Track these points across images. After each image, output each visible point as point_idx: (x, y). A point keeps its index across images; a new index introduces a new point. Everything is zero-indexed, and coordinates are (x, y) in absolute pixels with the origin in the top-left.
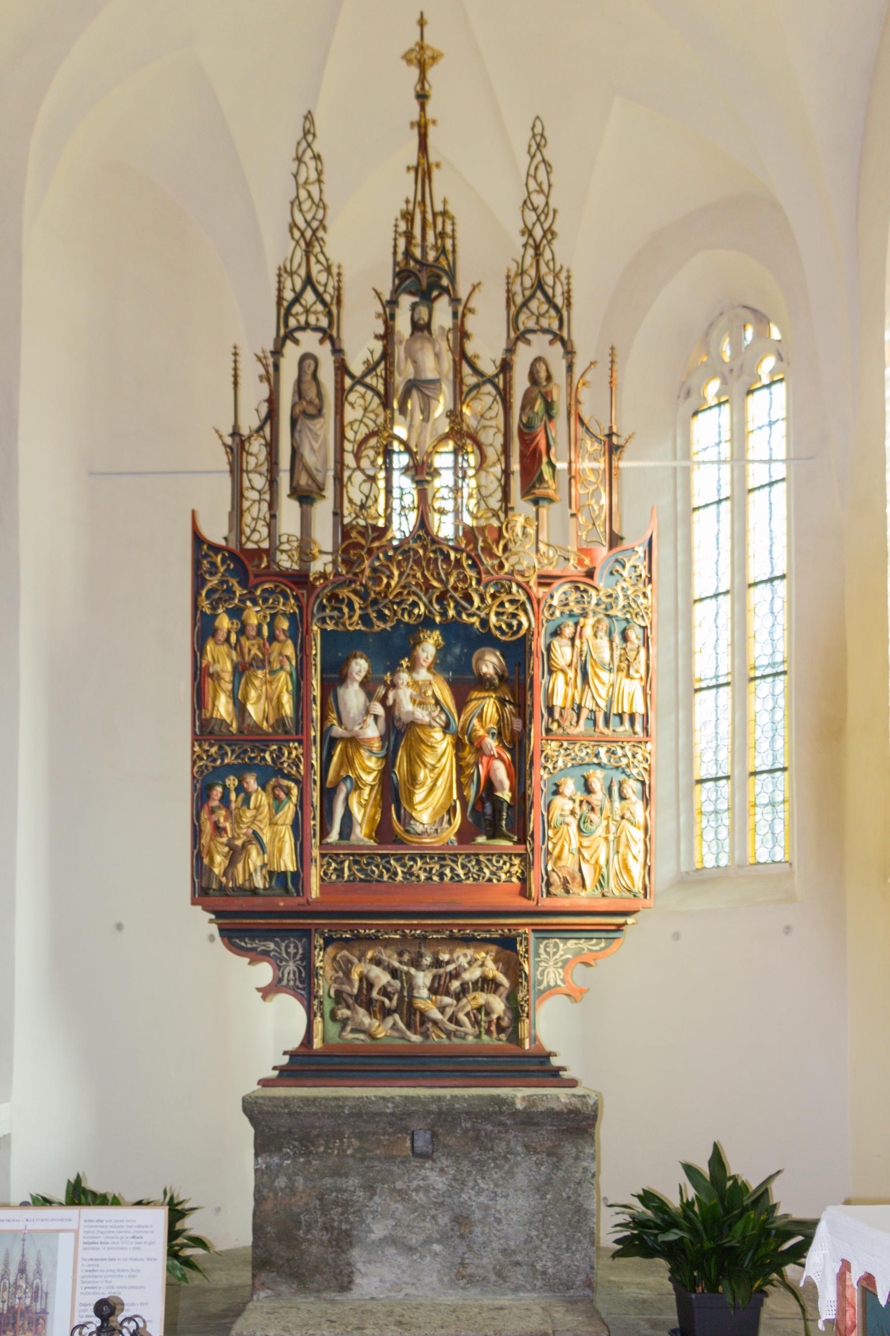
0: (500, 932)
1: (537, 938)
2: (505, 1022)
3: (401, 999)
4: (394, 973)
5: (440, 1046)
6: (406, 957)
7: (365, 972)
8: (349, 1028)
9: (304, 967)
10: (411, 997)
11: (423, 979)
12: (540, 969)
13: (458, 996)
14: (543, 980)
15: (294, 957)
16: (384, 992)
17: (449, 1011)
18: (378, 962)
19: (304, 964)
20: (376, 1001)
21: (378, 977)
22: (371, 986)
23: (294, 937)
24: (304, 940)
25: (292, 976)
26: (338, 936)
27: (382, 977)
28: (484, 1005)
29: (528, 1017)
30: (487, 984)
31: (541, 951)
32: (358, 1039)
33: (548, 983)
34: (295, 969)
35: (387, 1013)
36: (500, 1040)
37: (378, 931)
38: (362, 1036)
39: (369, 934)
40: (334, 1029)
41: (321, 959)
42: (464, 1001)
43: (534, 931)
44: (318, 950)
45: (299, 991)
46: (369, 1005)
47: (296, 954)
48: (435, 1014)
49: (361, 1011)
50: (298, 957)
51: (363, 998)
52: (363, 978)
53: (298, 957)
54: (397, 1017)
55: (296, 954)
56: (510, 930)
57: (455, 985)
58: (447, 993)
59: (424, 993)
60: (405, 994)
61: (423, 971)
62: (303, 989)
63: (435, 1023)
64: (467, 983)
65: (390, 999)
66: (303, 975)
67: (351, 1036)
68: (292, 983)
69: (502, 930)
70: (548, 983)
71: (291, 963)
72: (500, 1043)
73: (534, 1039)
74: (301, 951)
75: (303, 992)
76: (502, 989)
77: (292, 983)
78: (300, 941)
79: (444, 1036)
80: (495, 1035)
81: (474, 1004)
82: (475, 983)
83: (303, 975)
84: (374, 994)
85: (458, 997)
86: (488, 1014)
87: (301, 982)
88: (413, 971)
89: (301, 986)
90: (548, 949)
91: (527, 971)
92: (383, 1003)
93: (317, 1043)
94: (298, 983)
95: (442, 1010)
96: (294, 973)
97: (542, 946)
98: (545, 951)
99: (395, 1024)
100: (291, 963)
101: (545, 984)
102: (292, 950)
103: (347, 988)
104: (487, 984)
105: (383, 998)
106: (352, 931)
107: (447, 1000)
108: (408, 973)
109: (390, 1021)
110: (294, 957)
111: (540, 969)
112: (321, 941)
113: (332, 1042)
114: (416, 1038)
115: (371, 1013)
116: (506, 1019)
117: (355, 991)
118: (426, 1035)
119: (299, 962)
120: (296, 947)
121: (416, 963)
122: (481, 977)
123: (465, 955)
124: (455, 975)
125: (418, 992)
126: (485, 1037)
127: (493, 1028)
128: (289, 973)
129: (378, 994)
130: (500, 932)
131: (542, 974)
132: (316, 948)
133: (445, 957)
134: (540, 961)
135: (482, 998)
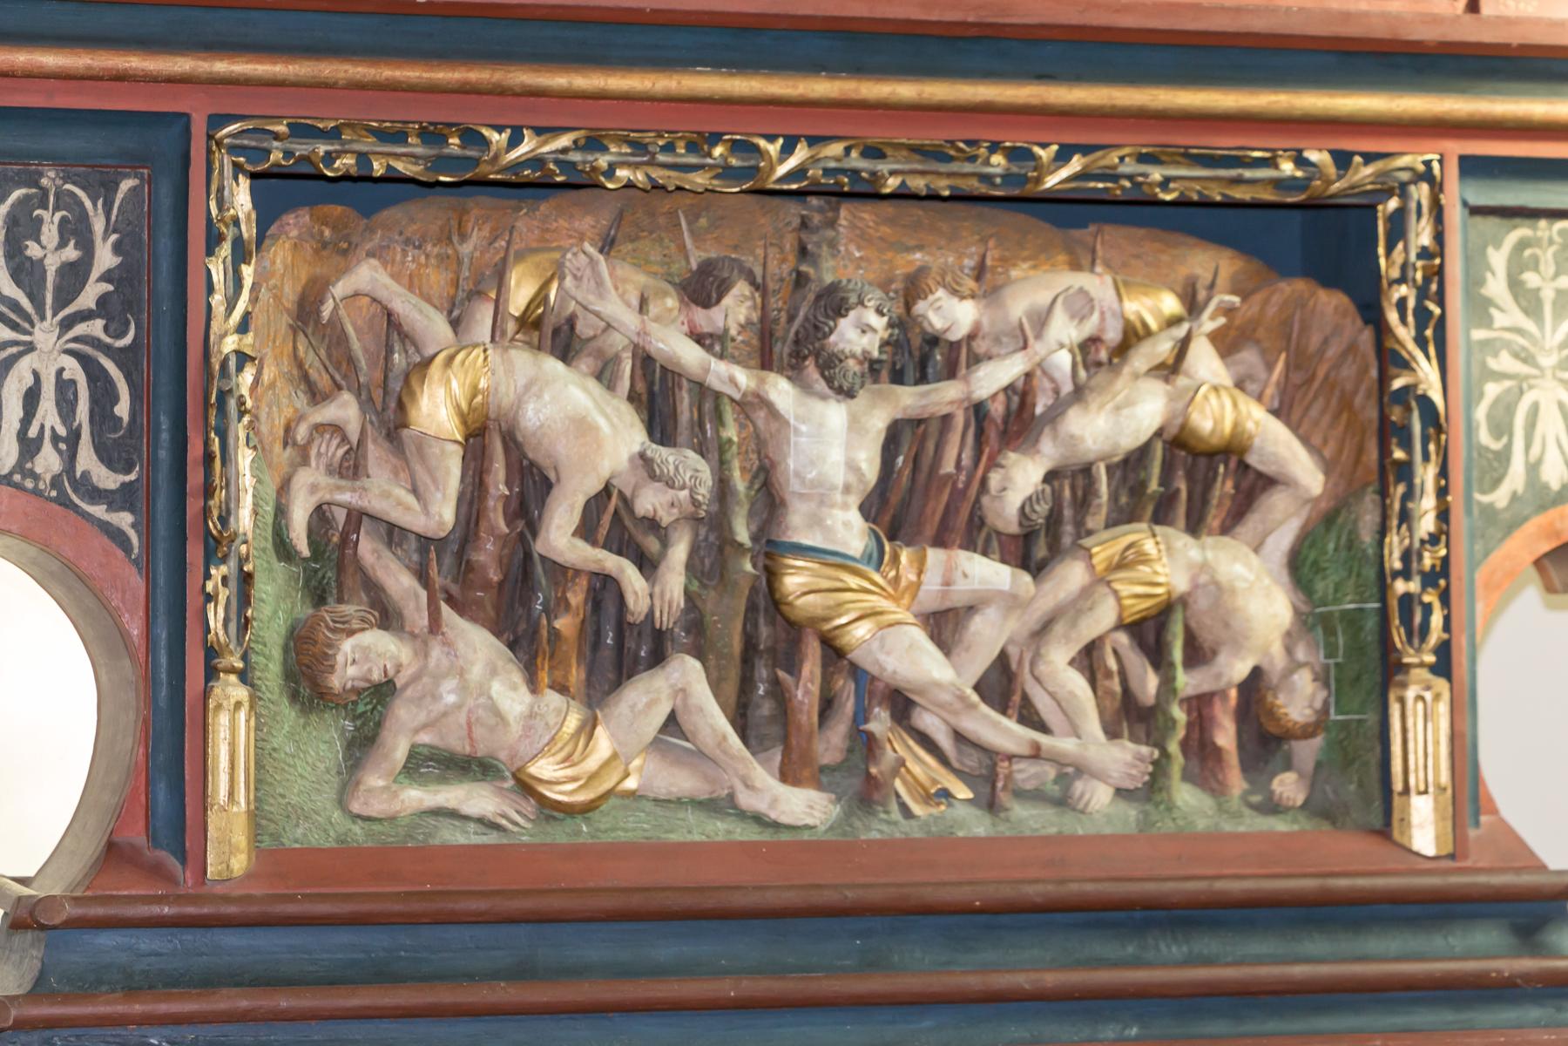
0: (1287, 168)
1: (1476, 211)
2: (1299, 700)
3: (711, 562)
4: (658, 397)
5: (945, 843)
6: (735, 309)
7: (506, 395)
8: (398, 748)
9: (124, 358)
10: (772, 552)
11: (832, 444)
12: (1492, 390)
13: (1032, 548)
14: (1504, 457)
15: (63, 299)
16: (611, 518)
17: (988, 635)
18: (557, 335)
19: (127, 340)
20: (560, 572)
21: (582, 427)
22: (534, 486)
23: (57, 160)
24: (126, 185)
25: (48, 414)
26: (346, 163)
27: (587, 428)
28: (1184, 601)
29: (1443, 666)
30: (1194, 479)
31: (1496, 286)
32: (454, 814)
33: (1533, 468)
34: (74, 370)
35: (618, 651)
36: (1272, 807)
37: (594, 143)
38: (478, 799)
39: (537, 162)
40: (317, 746)
41: (240, 306)
42: (1071, 576)
43: (1472, 167)
44: (225, 250)
45: (99, 511)
46: (509, 594)
47: (74, 275)
48: (910, 657)
49: (476, 644)
50: (88, 297)
51: (487, 554)
52: (484, 432)
53: (88, 297)
54: (687, 676)
55: (74, 275)
56: (1343, 160)
57: (1021, 480)
58: (974, 533)
59: (849, 530)
60: (743, 534)
61: (849, 394)
62: (121, 499)
63: (901, 704)
64: (1087, 470)
65: (648, 565)
66: (123, 409)
67: (416, 797)
68: (48, 461)
69: (1300, 161)
70: (1533, 468)
71: (45, 334)
72: (1279, 825)
73: (1467, 795)
74: (105, 258)
75: (124, 520)
76: (1277, 503)
77: (48, 461)
78: (104, 188)
79: (962, 792)
80: (1236, 782)
81: (1134, 593)
82: (1131, 464)
83: (123, 409)
84: (560, 536)
85: (1032, 548)
86: (1197, 654)
87: (106, 455)
88: (781, 391)
89: (108, 480)
90: (1531, 279)
91: (1436, 397)
92: (604, 588)
93: (229, 850)
94: (87, 459)
95: (944, 625)
96: (65, 388)
97: (1498, 259)
98: (1515, 285)
99: (672, 723)
100: (45, 334)
101: (1515, 478)
102: (50, 252)
103: (383, 492)
104: (1194, 479)
105: (612, 562)
106: (433, 135)
107: (985, 572)
108: (753, 405)
109: (646, 699)
110: (63, 299)
111: (1492, 390)
112: (242, 198)
113: (298, 835)
114: (804, 807)
115: (526, 645)
116: (1304, 681)
117: (443, 513)
118: (864, 787)
119: (96, 327)
120: (76, 230)
121: (795, 341)
122: (1159, 433)
123: (1082, 306)
124: (1017, 420)
125: (816, 521)
126: (1186, 796)
127: (1226, 736)
128: (31, 398)
129: (586, 530)
130: (1287, 168)
131: (1501, 427)
132: (213, 241)
133: (950, 314)
134: (1489, 346)
135: (1170, 561)
